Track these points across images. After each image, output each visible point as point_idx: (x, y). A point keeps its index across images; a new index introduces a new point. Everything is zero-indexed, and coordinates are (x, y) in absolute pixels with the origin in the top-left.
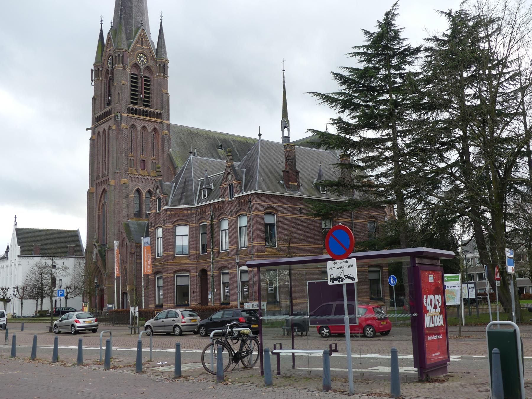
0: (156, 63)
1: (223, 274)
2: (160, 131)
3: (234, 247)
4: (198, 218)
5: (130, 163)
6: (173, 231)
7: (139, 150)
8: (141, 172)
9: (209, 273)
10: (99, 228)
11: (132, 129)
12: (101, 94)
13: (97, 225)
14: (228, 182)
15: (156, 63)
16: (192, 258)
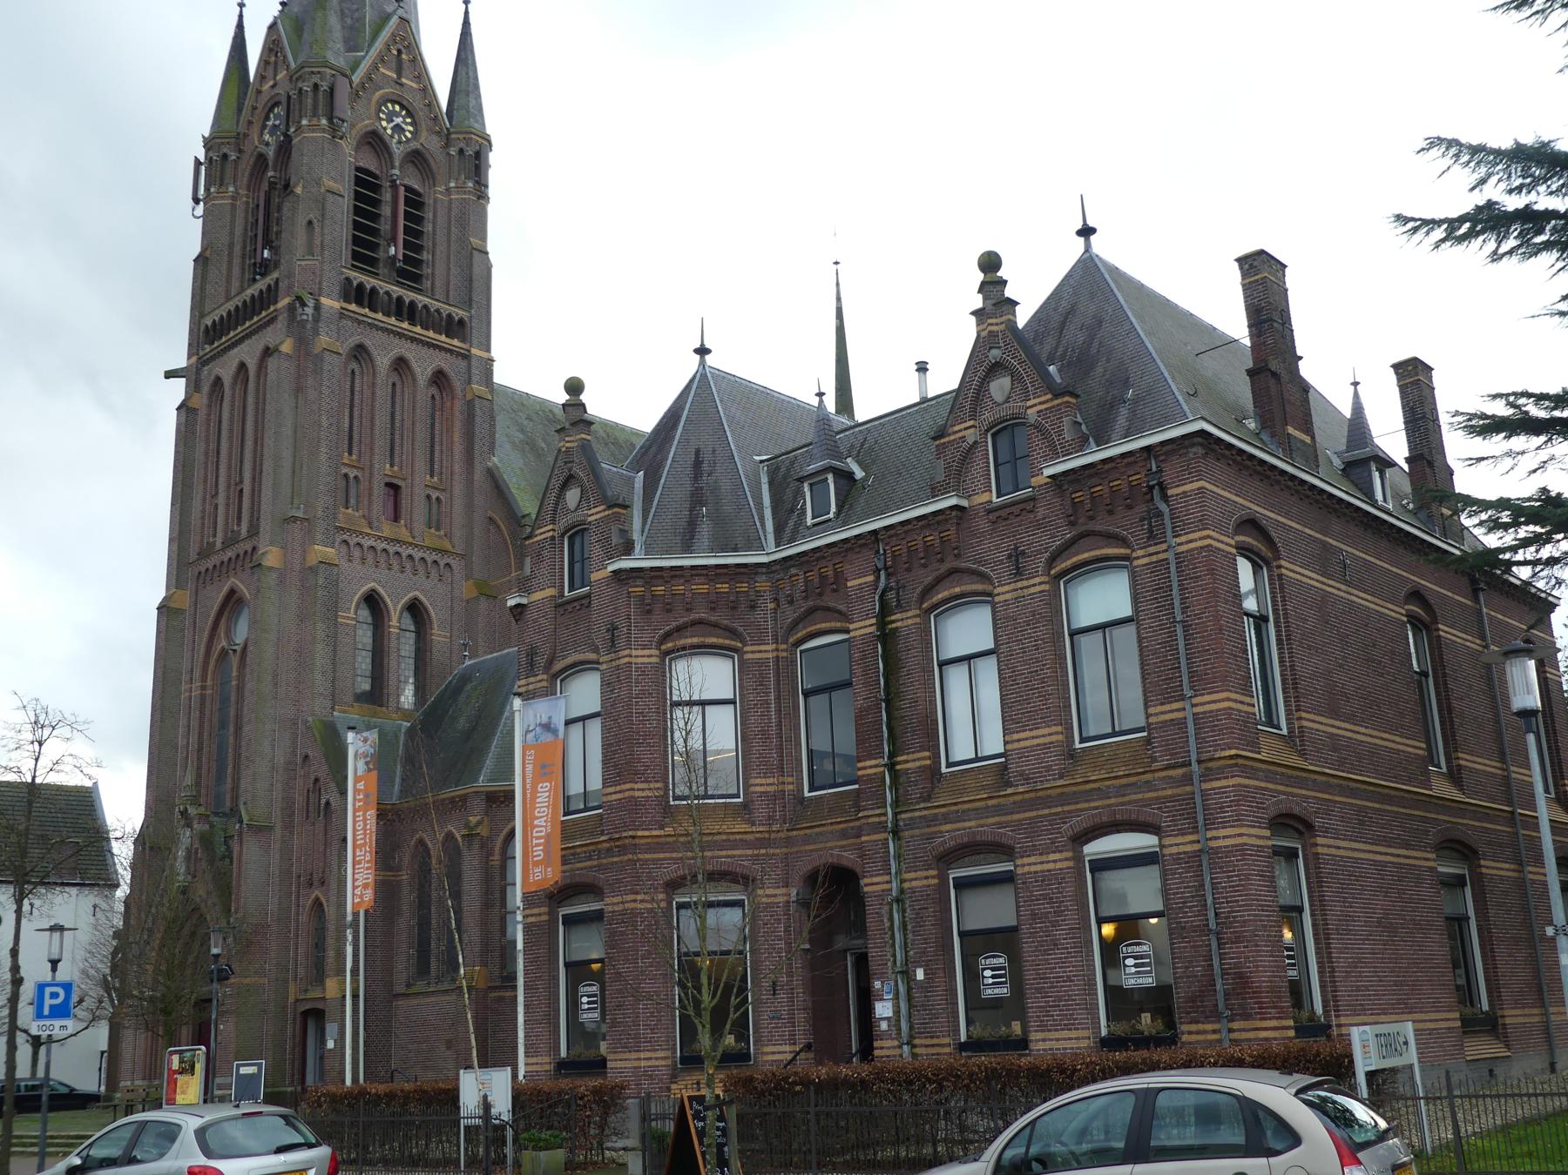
0: (447, 145)
1: (961, 884)
2: (457, 384)
3: (1047, 734)
4: (790, 614)
5: (347, 489)
6: (659, 677)
7: (381, 444)
8: (387, 529)
9: (872, 884)
10: (200, 749)
11: (354, 365)
12: (231, 246)
13: (194, 739)
14: (988, 416)
15: (447, 145)
16: (761, 811)
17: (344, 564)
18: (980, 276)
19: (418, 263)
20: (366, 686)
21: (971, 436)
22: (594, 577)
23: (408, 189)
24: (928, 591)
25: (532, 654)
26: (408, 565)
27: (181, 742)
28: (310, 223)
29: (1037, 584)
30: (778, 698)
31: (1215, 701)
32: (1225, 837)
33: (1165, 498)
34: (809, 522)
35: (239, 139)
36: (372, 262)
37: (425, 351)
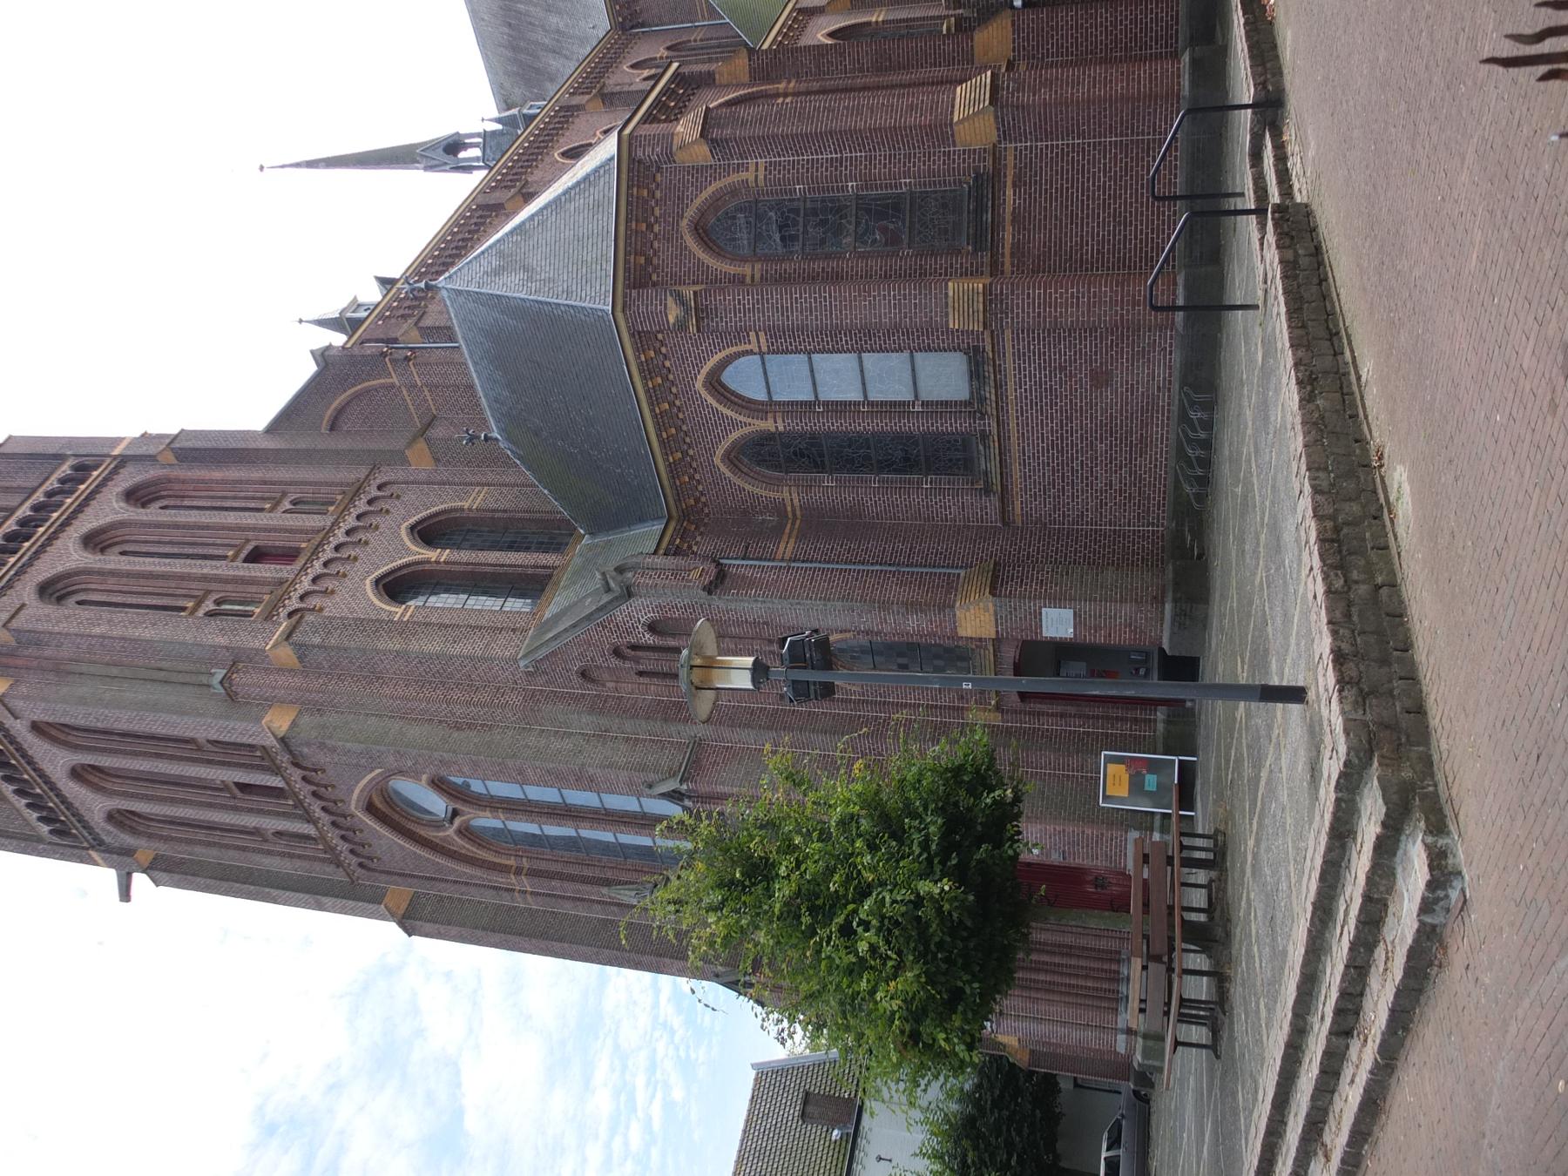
2: (152, 473)
37: (89, 511)
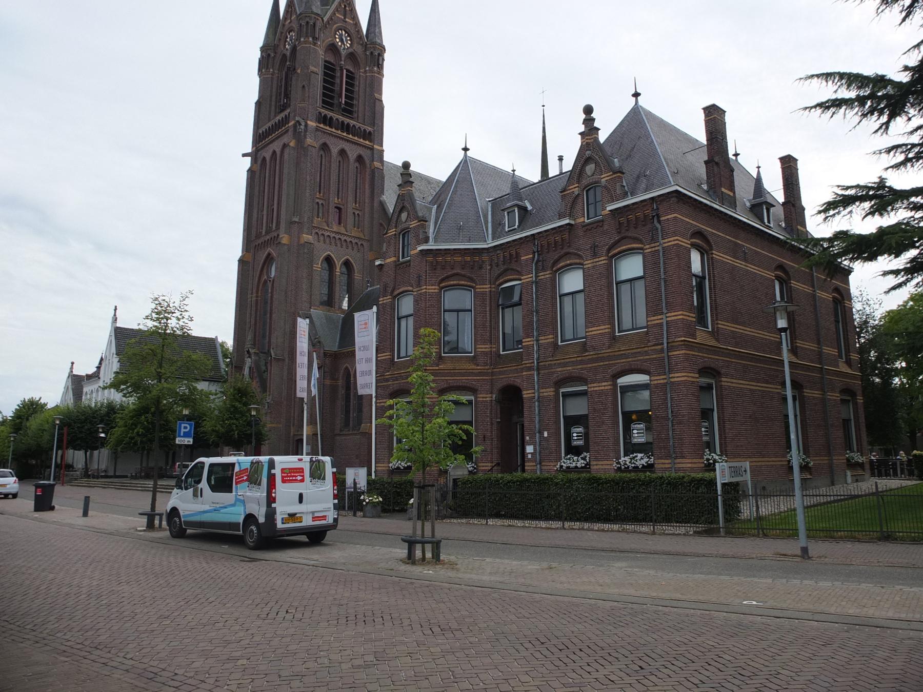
0: (366, 50)
1: (565, 395)
2: (367, 162)
3: (604, 329)
4: (497, 271)
6: (438, 298)
7: (333, 188)
9: (526, 394)
11: (322, 152)
12: (271, 97)
14: (584, 182)
15: (366, 50)
17: (316, 243)
18: (584, 116)
19: (352, 105)
20: (326, 298)
21: (576, 191)
22: (413, 252)
23: (347, 71)
24: (556, 262)
25: (385, 287)
26: (344, 244)
27: (248, 320)
28: (304, 86)
29: (602, 260)
30: (490, 310)
31: (677, 315)
32: (678, 377)
33: (659, 222)
34: (507, 229)
35: (275, 48)
36: (331, 105)
